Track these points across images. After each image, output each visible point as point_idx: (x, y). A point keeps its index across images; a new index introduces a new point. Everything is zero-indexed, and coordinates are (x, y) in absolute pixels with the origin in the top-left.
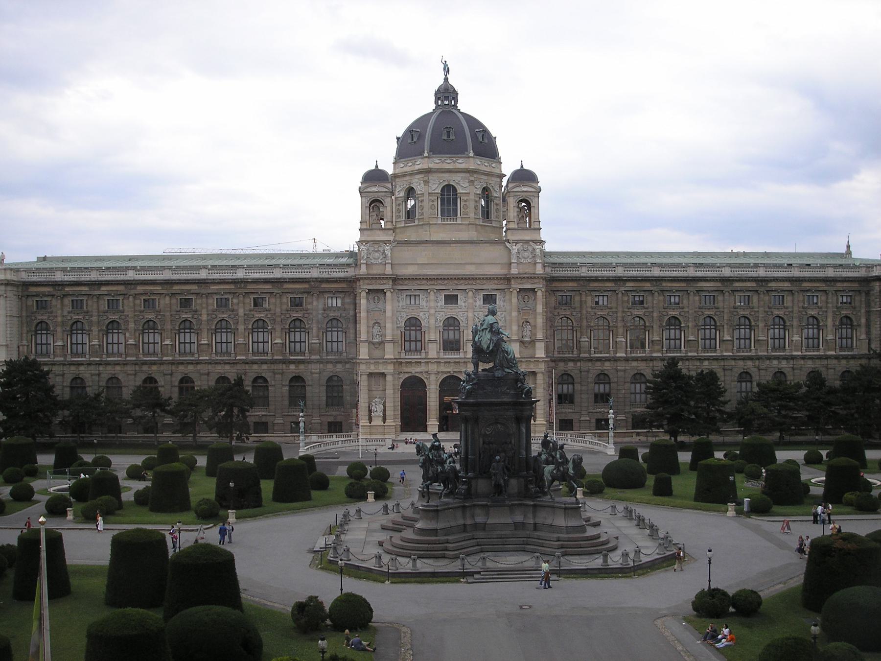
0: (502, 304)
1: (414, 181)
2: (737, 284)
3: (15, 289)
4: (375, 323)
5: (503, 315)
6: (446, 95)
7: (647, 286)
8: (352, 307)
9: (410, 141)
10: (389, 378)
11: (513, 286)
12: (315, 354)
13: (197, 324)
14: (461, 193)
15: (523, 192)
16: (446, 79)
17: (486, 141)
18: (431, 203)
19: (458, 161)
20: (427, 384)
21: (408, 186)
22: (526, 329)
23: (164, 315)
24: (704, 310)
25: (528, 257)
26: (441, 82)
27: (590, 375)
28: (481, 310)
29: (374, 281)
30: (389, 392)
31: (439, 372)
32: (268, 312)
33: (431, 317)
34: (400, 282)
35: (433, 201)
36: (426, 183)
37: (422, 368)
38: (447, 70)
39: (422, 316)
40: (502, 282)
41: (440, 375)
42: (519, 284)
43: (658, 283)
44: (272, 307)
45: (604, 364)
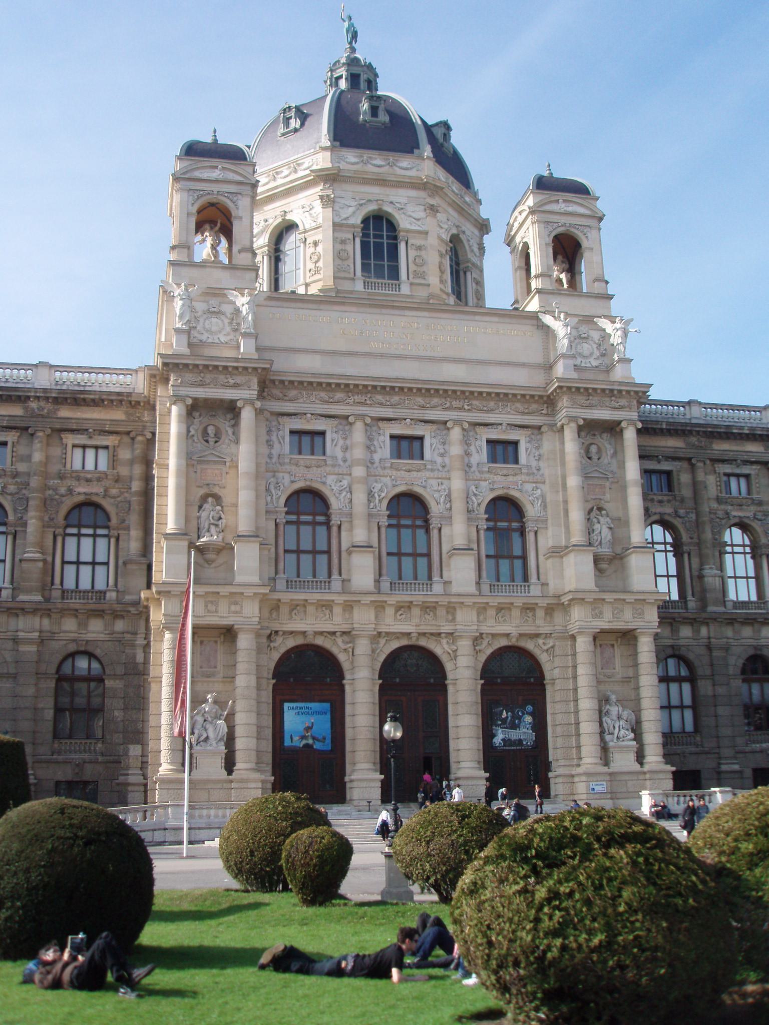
0: (534, 464)
1: (293, 206)
4: (204, 499)
5: (539, 491)
6: (355, 70)
8: (138, 470)
10: (244, 642)
12: (29, 591)
14: (408, 231)
16: (353, 50)
18: (339, 247)
20: (346, 666)
21: (280, 220)
22: (597, 527)
25: (591, 354)
27: (732, 660)
28: (483, 476)
29: (208, 377)
30: (244, 681)
31: (380, 633)
33: (355, 487)
34: (276, 392)
37: (337, 621)
38: (355, 36)
39: (331, 487)
40: (534, 406)
41: (382, 641)
42: (582, 407)
45: (759, 631)
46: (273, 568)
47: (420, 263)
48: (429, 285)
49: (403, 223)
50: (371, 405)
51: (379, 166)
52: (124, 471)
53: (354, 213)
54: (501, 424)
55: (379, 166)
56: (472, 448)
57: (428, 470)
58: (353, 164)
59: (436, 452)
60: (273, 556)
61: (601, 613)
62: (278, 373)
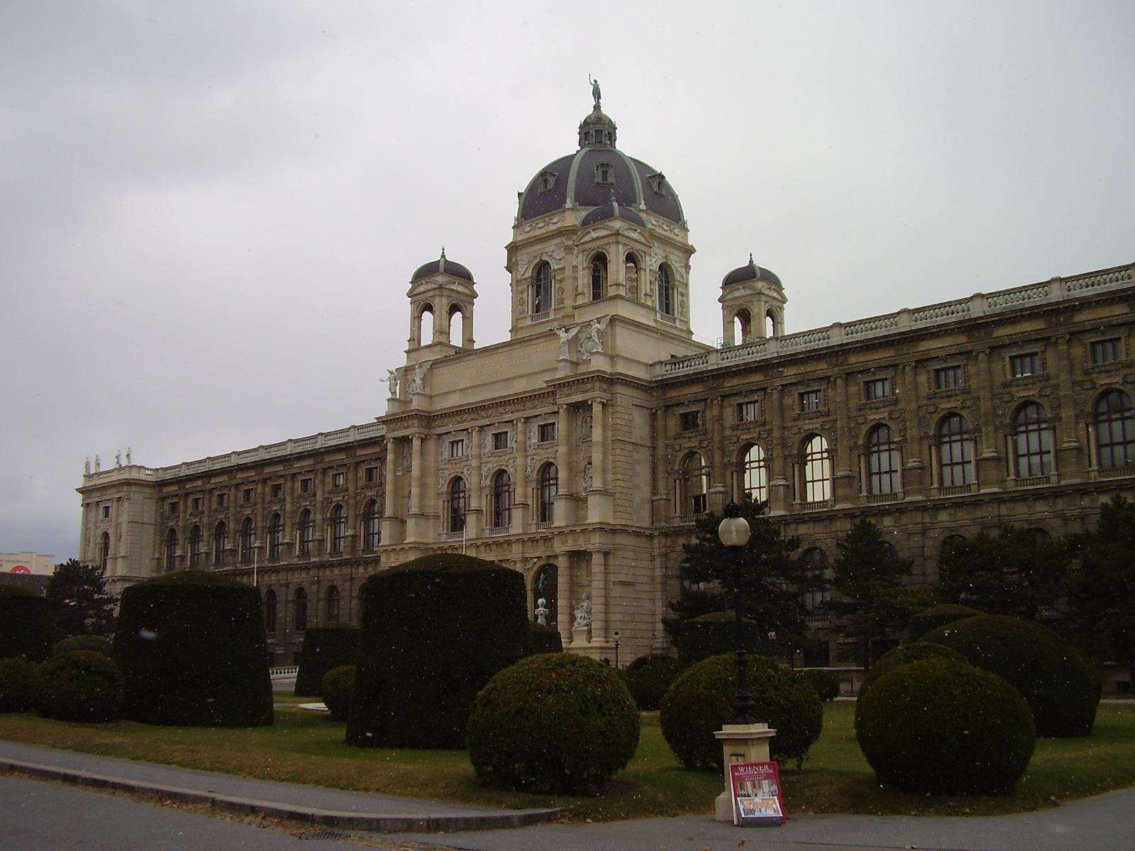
2: (1001, 332)
3: (147, 490)
6: (586, 130)
7: (821, 368)
11: (559, 401)
14: (555, 270)
15: (597, 239)
16: (597, 107)
17: (611, 180)
18: (520, 296)
19: (554, 221)
24: (938, 401)
26: (590, 111)
38: (597, 94)
43: (841, 359)
46: (441, 528)
47: (562, 290)
48: (563, 308)
49: (554, 266)
50: (477, 419)
51: (542, 227)
53: (527, 269)
54: (541, 415)
55: (542, 227)
56: (532, 434)
57: (509, 453)
58: (528, 232)
59: (514, 439)
60: (441, 521)
61: (566, 541)
62: (437, 411)
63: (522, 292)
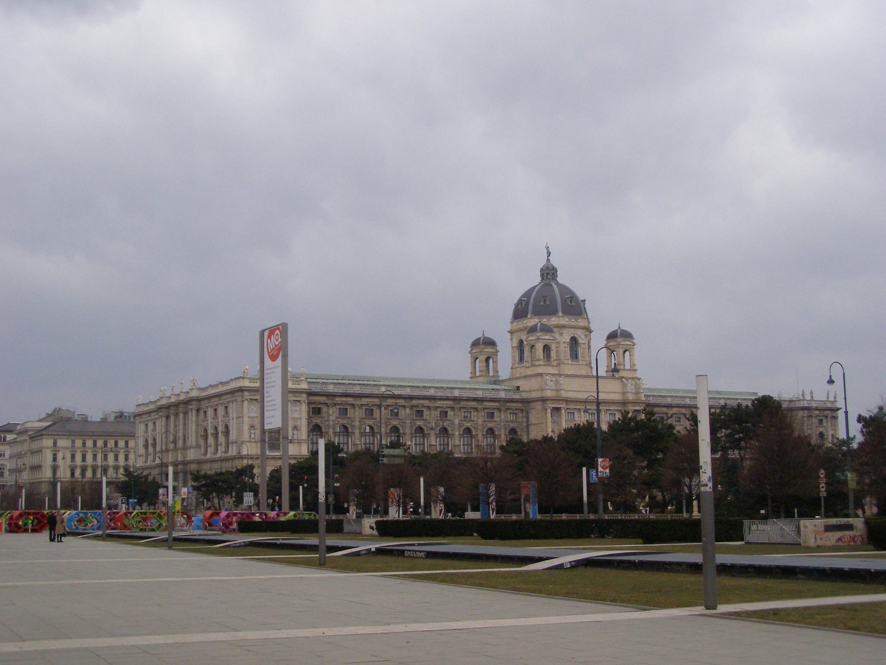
8: (525, 420)
9: (542, 303)
13: (427, 430)
16: (548, 260)
18: (564, 349)
23: (405, 422)
32: (472, 423)
35: (565, 347)
36: (561, 334)
38: (549, 254)
44: (475, 419)
49: (580, 341)
52: (520, 420)
63: (565, 347)
